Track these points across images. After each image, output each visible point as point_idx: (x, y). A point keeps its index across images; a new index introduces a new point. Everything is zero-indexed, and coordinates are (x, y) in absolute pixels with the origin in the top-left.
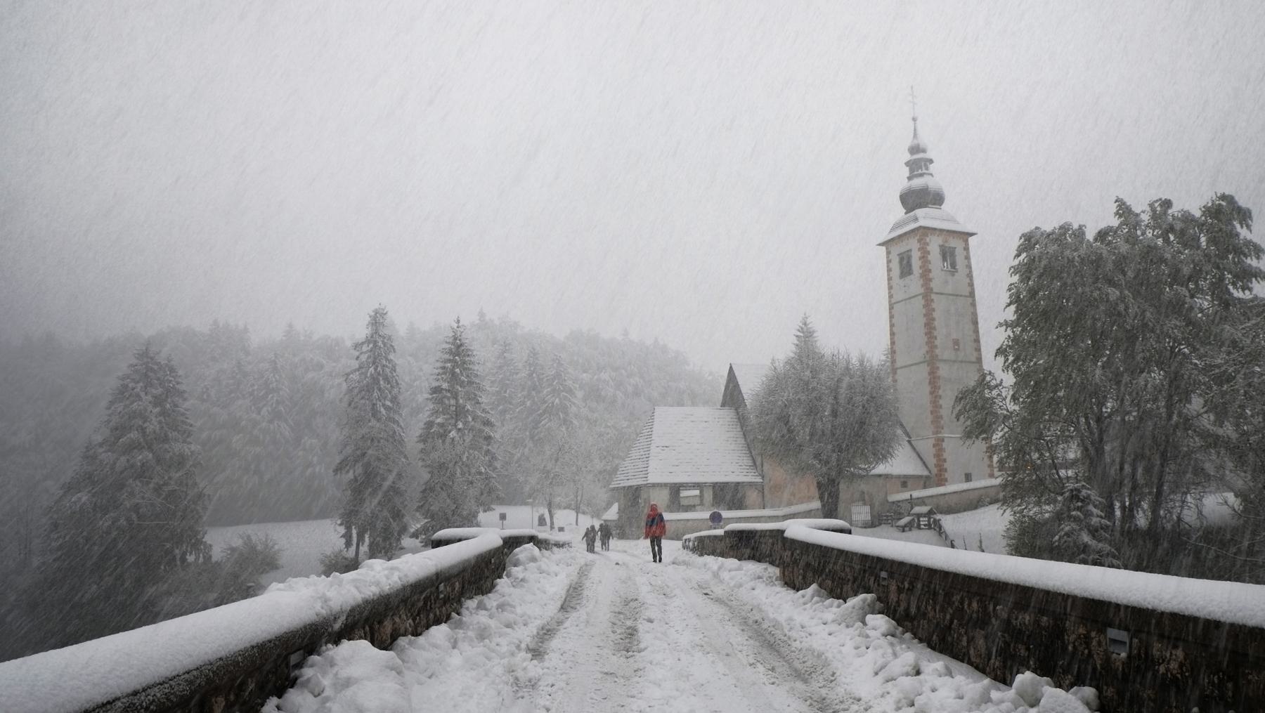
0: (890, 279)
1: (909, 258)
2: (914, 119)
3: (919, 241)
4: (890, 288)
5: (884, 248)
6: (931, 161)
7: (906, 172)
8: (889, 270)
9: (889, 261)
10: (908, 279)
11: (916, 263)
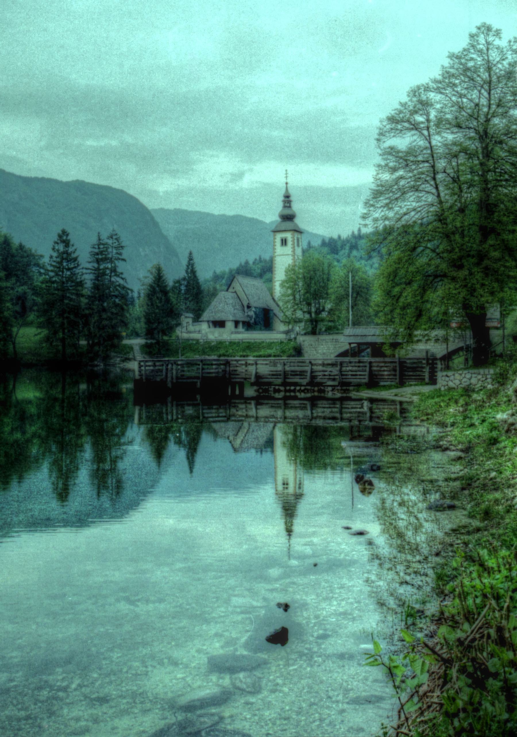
10: (284, 248)
11: (290, 243)
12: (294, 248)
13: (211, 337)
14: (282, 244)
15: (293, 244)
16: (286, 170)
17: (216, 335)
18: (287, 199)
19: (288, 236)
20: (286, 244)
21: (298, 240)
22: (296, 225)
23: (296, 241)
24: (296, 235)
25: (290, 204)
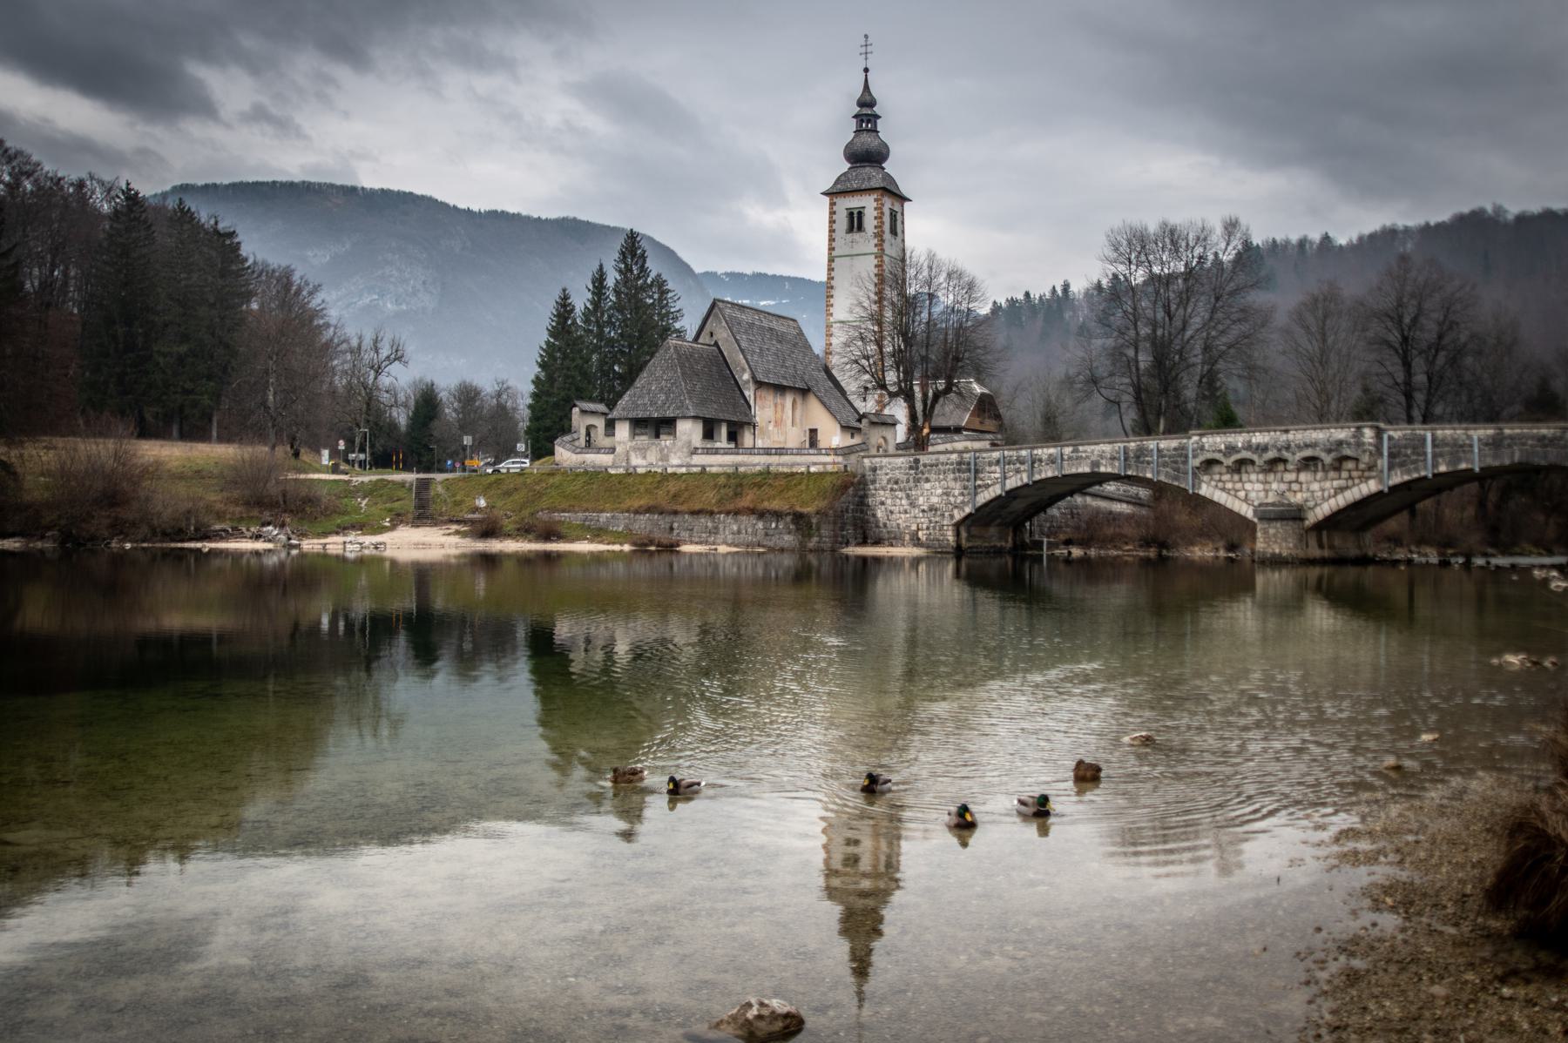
0: (832, 231)
1: (860, 214)
2: (866, 70)
3: (876, 200)
4: (831, 240)
5: (827, 199)
6: (879, 117)
7: (853, 125)
8: (832, 222)
9: (832, 213)
10: (856, 236)
11: (870, 222)
12: (879, 235)
13: (639, 463)
14: (851, 229)
15: (880, 226)
16: (866, 36)
17: (652, 457)
18: (867, 113)
19: (868, 203)
20: (860, 228)
21: (893, 215)
22: (888, 177)
23: (887, 219)
24: (888, 203)
25: (876, 126)
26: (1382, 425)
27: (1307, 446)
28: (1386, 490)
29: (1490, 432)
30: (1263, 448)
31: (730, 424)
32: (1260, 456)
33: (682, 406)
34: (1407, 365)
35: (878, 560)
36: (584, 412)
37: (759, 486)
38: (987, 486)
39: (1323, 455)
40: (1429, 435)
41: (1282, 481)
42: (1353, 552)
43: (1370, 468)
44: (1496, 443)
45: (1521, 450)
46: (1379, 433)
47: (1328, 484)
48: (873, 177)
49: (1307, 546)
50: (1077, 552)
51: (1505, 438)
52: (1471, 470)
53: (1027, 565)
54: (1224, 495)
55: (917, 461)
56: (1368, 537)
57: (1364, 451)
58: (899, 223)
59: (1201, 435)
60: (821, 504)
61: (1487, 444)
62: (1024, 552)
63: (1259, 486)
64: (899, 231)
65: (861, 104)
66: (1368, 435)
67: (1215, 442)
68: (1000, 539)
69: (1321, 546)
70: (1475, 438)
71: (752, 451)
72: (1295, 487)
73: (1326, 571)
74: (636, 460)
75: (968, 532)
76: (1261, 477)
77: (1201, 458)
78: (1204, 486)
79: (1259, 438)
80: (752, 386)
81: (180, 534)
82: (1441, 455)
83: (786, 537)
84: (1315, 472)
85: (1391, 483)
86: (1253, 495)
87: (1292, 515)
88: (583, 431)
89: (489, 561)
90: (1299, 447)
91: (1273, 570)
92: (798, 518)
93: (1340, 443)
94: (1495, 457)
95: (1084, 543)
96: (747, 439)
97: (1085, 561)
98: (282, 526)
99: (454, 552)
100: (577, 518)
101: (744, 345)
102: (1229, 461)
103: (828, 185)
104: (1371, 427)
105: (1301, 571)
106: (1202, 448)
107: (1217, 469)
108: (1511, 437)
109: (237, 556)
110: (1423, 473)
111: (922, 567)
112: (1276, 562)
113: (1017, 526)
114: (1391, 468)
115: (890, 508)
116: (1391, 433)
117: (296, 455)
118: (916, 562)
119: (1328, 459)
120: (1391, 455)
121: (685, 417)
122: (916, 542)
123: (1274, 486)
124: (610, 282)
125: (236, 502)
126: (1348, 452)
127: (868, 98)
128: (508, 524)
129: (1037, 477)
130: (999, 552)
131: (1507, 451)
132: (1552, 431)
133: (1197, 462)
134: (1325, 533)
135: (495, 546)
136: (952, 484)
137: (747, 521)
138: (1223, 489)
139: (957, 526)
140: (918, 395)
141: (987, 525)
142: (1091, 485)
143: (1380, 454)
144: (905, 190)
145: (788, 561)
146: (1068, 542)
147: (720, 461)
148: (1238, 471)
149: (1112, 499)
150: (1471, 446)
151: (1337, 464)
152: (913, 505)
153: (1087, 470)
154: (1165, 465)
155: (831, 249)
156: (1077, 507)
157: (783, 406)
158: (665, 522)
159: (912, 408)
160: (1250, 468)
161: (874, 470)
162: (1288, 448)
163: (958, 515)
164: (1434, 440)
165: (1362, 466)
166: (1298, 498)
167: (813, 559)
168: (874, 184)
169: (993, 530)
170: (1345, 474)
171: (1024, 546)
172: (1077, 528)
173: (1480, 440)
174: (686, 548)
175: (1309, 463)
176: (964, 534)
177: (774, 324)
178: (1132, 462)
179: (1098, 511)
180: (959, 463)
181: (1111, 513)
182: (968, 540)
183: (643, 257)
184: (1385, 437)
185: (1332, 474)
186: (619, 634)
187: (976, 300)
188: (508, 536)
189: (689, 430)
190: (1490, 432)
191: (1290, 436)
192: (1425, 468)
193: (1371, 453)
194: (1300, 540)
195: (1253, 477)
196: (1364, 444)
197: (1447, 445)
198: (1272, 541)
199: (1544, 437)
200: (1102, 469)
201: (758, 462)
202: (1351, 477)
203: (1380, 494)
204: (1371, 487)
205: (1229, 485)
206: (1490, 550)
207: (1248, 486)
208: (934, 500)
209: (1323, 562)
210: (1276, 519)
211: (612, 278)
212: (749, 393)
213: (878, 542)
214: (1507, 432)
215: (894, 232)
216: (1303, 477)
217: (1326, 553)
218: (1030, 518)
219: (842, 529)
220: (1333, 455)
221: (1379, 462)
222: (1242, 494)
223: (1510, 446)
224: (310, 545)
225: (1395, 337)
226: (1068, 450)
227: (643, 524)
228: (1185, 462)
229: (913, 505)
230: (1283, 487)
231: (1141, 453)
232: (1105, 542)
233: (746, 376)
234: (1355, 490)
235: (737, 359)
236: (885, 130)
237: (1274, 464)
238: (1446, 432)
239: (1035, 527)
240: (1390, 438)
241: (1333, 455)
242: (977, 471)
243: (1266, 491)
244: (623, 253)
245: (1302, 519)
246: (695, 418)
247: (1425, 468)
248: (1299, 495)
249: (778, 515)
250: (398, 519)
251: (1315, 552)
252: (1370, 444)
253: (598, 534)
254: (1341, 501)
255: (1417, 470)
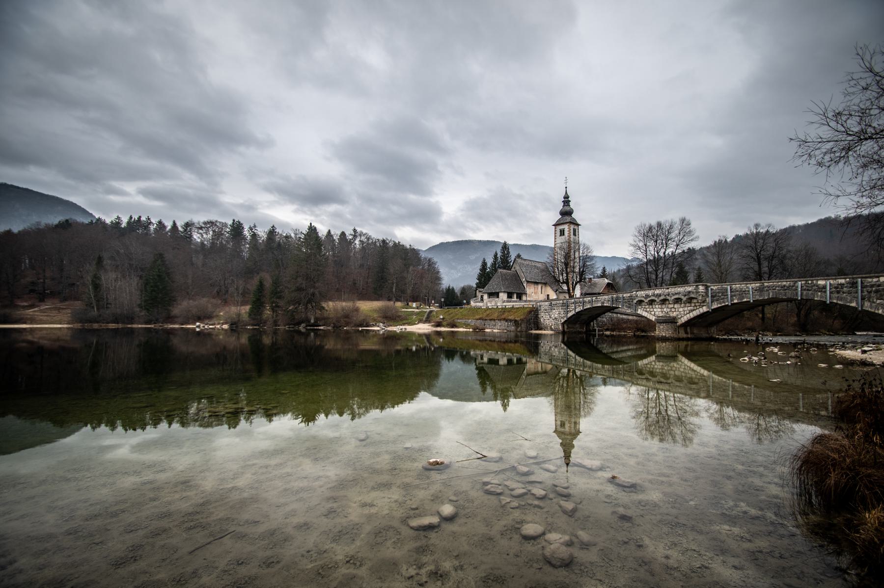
0: (555, 236)
1: (564, 230)
2: (566, 188)
4: (555, 239)
8: (555, 233)
9: (555, 231)
10: (563, 237)
11: (566, 233)
14: (561, 235)
15: (569, 233)
17: (493, 304)
18: (566, 201)
19: (566, 227)
20: (564, 235)
22: (574, 220)
23: (572, 231)
24: (572, 227)
26: (709, 284)
27: (676, 294)
28: (710, 311)
29: (758, 285)
30: (660, 295)
31: (517, 294)
32: (658, 298)
33: (501, 289)
34: (760, 264)
35: (541, 335)
36: (480, 291)
37: (509, 311)
38: (571, 311)
39: (682, 297)
40: (729, 287)
41: (668, 308)
42: (705, 335)
43: (704, 302)
44: (761, 290)
45: (773, 292)
46: (707, 287)
47: (686, 309)
48: (568, 219)
49: (679, 333)
50: (608, 333)
51: (766, 287)
52: (749, 301)
53: (591, 337)
54: (647, 313)
55: (551, 303)
56: (713, 329)
57: (700, 295)
58: (577, 232)
59: (637, 291)
60: (522, 317)
61: (756, 290)
62: (590, 333)
63: (659, 310)
64: (577, 234)
65: (564, 198)
66: (701, 288)
67: (641, 294)
68: (581, 328)
69: (686, 333)
70: (750, 287)
71: (526, 301)
72: (673, 310)
73: (689, 343)
74: (489, 305)
75: (568, 326)
76: (660, 306)
77: (637, 300)
78: (639, 310)
79: (657, 292)
80: (526, 282)
81: (361, 325)
82: (735, 296)
83: (513, 327)
84: (681, 304)
85: (712, 308)
86: (657, 313)
87: (672, 321)
88: (480, 297)
89: (439, 333)
90: (673, 295)
91: (662, 342)
92: (516, 321)
93: (689, 292)
94: (760, 296)
95: (613, 330)
96: (524, 298)
97: (612, 336)
98: (384, 323)
99: (430, 331)
100: (463, 321)
101: (523, 270)
102: (646, 301)
103: (554, 223)
104: (703, 285)
105: (676, 343)
106: (637, 296)
107: (643, 304)
108: (768, 287)
109: (374, 331)
110: (727, 303)
111: (553, 336)
112: (664, 339)
113: (588, 324)
114: (712, 302)
115: (545, 318)
116: (712, 287)
117: (408, 304)
118: (551, 335)
119: (684, 299)
120: (712, 296)
121: (501, 292)
122: (552, 329)
123: (665, 310)
124: (498, 256)
125: (380, 317)
126: (693, 296)
127: (566, 196)
128: (444, 323)
129: (585, 308)
130: (580, 333)
131: (766, 293)
132: (788, 283)
133: (635, 301)
134: (688, 328)
135: (439, 329)
136: (561, 310)
137: (503, 322)
138: (646, 311)
139: (563, 324)
140: (570, 283)
141: (575, 323)
142: (611, 310)
143: (708, 296)
144: (579, 222)
145: (513, 334)
146: (607, 330)
147: (515, 303)
148: (652, 305)
149: (629, 315)
150: (749, 291)
151: (689, 301)
152: (550, 317)
153: (600, 305)
154: (626, 303)
155: (555, 241)
156: (614, 318)
157: (537, 288)
158: (483, 322)
159: (568, 287)
160: (656, 303)
161: (540, 306)
162: (668, 295)
163: (563, 321)
164: (731, 290)
165: (699, 301)
166: (675, 314)
167: (518, 333)
168: (568, 221)
169: (577, 326)
170: (693, 305)
171: (590, 331)
172: (613, 325)
173: (752, 288)
174: (487, 330)
175: (678, 301)
176: (566, 327)
177: (537, 264)
178: (615, 302)
179: (623, 319)
180: (563, 304)
181: (628, 319)
182: (567, 329)
183: (508, 248)
184: (710, 289)
185: (688, 305)
186: (485, 355)
187: (589, 252)
188: (444, 326)
189: (503, 296)
190: (758, 285)
191: (670, 290)
192: (728, 301)
193: (702, 296)
194: (675, 330)
195: (657, 306)
196: (699, 292)
197: (737, 291)
198: (662, 331)
199: (785, 286)
200: (605, 305)
201: (526, 305)
202: (695, 306)
203: (708, 312)
204: (705, 309)
205: (648, 310)
206: (798, 333)
207: (655, 310)
208: (556, 316)
209: (687, 339)
210: (664, 323)
211: (499, 255)
212: (525, 285)
213: (541, 329)
214: (766, 284)
215: (575, 234)
216: (676, 306)
217: (689, 336)
218: (592, 321)
219: (530, 325)
220: (687, 297)
221: (707, 299)
222: (653, 313)
223: (767, 290)
224: (390, 329)
225: (753, 255)
226: (594, 298)
227: (479, 323)
228: (632, 302)
229: (550, 317)
230: (669, 310)
231: (617, 298)
232: (620, 330)
233: (524, 280)
234: (697, 310)
235: (521, 275)
236: (572, 205)
237: (664, 301)
238: (737, 286)
239: (594, 324)
240: (712, 289)
241: (687, 297)
242: (568, 306)
243: (662, 312)
244: (502, 248)
245: (676, 323)
246: (504, 292)
247: (728, 301)
248: (675, 313)
249: (511, 321)
250: (420, 321)
251: (682, 335)
252: (702, 292)
253: (467, 325)
254: (692, 315)
255: (724, 302)
